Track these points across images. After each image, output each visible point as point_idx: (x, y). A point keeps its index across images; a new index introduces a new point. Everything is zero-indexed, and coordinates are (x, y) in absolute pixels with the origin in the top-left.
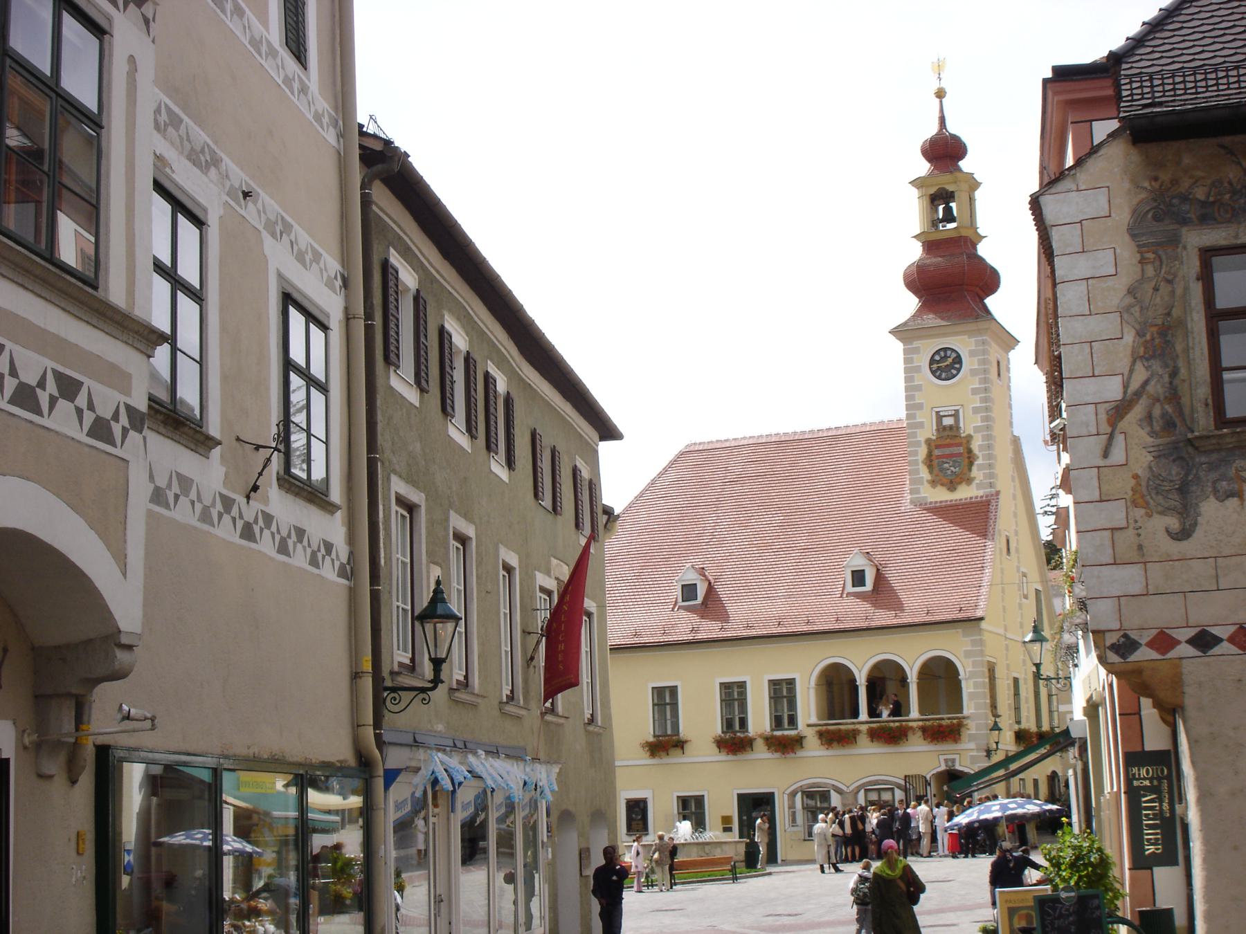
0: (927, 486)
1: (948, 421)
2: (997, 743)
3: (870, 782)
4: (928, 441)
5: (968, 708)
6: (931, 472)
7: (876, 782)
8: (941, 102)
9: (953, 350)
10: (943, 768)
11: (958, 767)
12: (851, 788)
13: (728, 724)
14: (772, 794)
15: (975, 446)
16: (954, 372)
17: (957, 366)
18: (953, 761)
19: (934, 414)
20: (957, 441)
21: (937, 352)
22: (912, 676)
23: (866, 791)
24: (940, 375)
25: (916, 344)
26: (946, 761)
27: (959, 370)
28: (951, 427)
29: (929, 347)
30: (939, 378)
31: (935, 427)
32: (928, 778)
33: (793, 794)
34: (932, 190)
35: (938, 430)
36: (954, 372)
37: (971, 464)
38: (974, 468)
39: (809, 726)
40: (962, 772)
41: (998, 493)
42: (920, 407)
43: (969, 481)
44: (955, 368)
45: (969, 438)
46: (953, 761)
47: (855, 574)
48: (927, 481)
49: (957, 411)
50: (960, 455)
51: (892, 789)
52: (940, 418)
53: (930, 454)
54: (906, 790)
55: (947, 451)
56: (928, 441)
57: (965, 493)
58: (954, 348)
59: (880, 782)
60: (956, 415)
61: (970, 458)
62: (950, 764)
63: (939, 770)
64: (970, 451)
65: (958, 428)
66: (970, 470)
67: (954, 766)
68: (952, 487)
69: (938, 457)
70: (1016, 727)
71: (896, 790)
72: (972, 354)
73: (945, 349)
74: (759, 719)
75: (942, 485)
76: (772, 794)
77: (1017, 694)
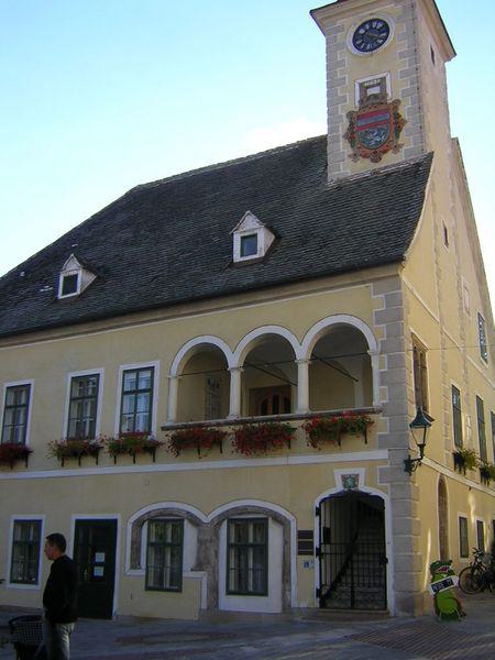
0: (349, 161)
1: (371, 92)
2: (422, 447)
4: (350, 115)
5: (379, 397)
6: (352, 147)
9: (379, 21)
10: (339, 488)
11: (363, 487)
12: (210, 518)
15: (403, 111)
17: (385, 34)
18: (355, 478)
19: (357, 87)
20: (383, 107)
21: (362, 26)
22: (302, 352)
23: (231, 521)
24: (365, 46)
26: (344, 478)
27: (385, 39)
28: (375, 96)
29: (350, 24)
30: (364, 50)
31: (358, 99)
33: (139, 524)
35: (361, 101)
36: (381, 41)
37: (398, 130)
38: (403, 133)
39: (164, 429)
40: (367, 495)
41: (431, 156)
43: (397, 148)
45: (397, 102)
46: (355, 478)
47: (246, 240)
48: (350, 156)
49: (383, 79)
50: (386, 122)
52: (364, 88)
53: (352, 124)
55: (370, 121)
56: (350, 115)
57: (391, 160)
58: (380, 18)
60: (382, 83)
61: (398, 124)
62: (350, 482)
63: (334, 491)
64: (397, 116)
65: (383, 95)
66: (398, 136)
67: (355, 486)
68: (376, 159)
69: (361, 128)
70: (455, 449)
74: (108, 425)
75: (365, 156)
77: (457, 410)
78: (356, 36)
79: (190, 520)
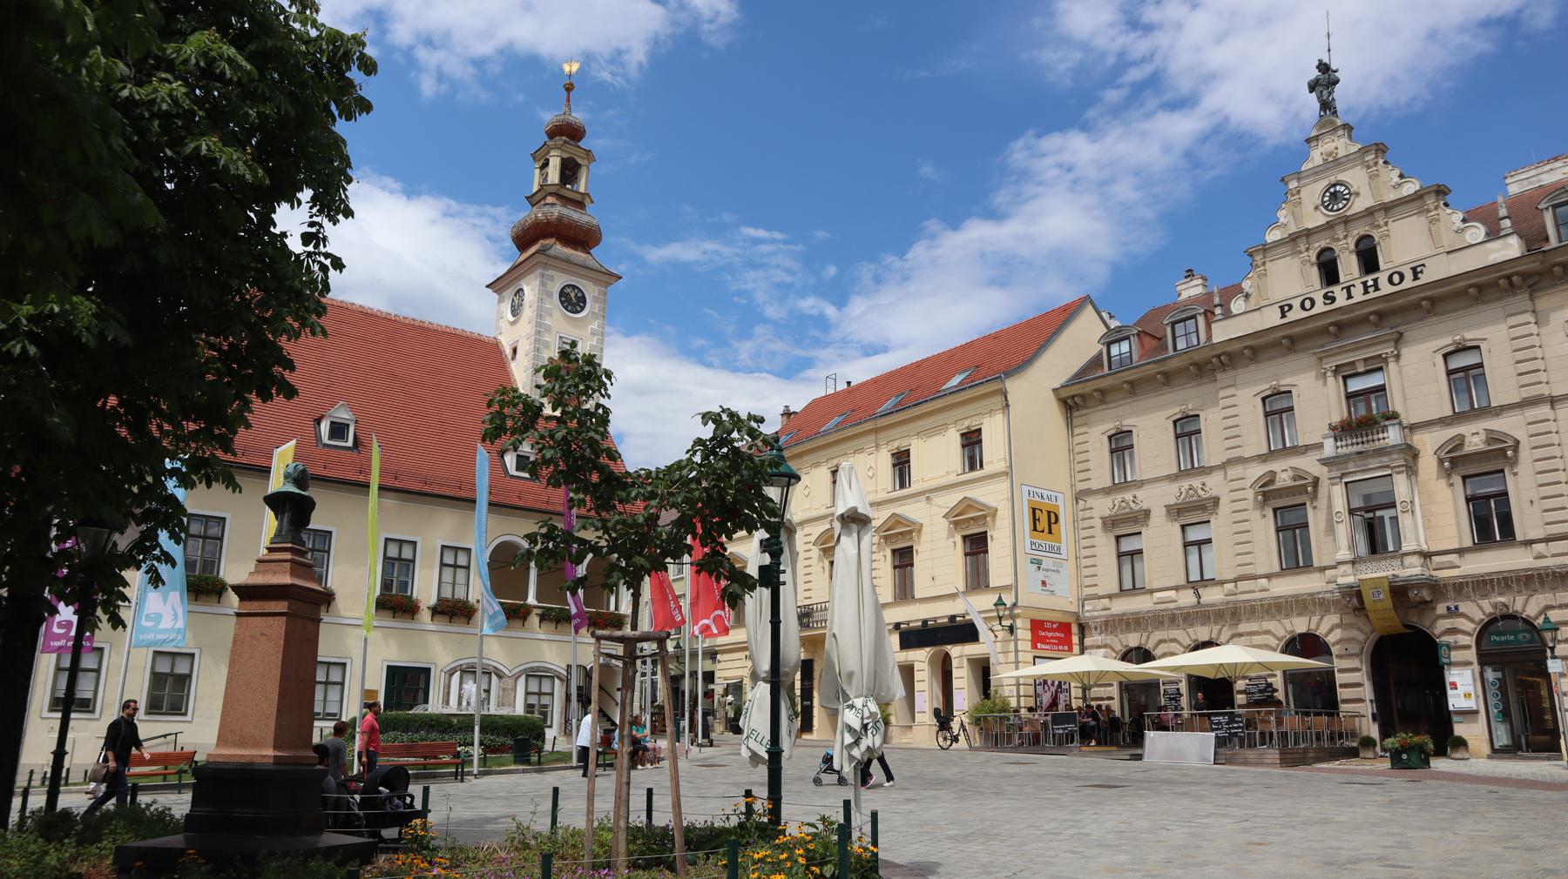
3: (532, 668)
7: (538, 669)
8: (569, 94)
9: (582, 292)
13: (386, 585)
14: (426, 672)
16: (579, 309)
21: (568, 286)
23: (528, 676)
25: (550, 272)
27: (583, 309)
30: (566, 308)
32: (588, 668)
34: (566, 156)
42: (548, 329)
44: (580, 306)
51: (553, 677)
54: (567, 681)
59: (542, 669)
71: (557, 681)
72: (595, 299)
73: (574, 287)
76: (426, 672)
78: (563, 294)
79: (496, 674)
